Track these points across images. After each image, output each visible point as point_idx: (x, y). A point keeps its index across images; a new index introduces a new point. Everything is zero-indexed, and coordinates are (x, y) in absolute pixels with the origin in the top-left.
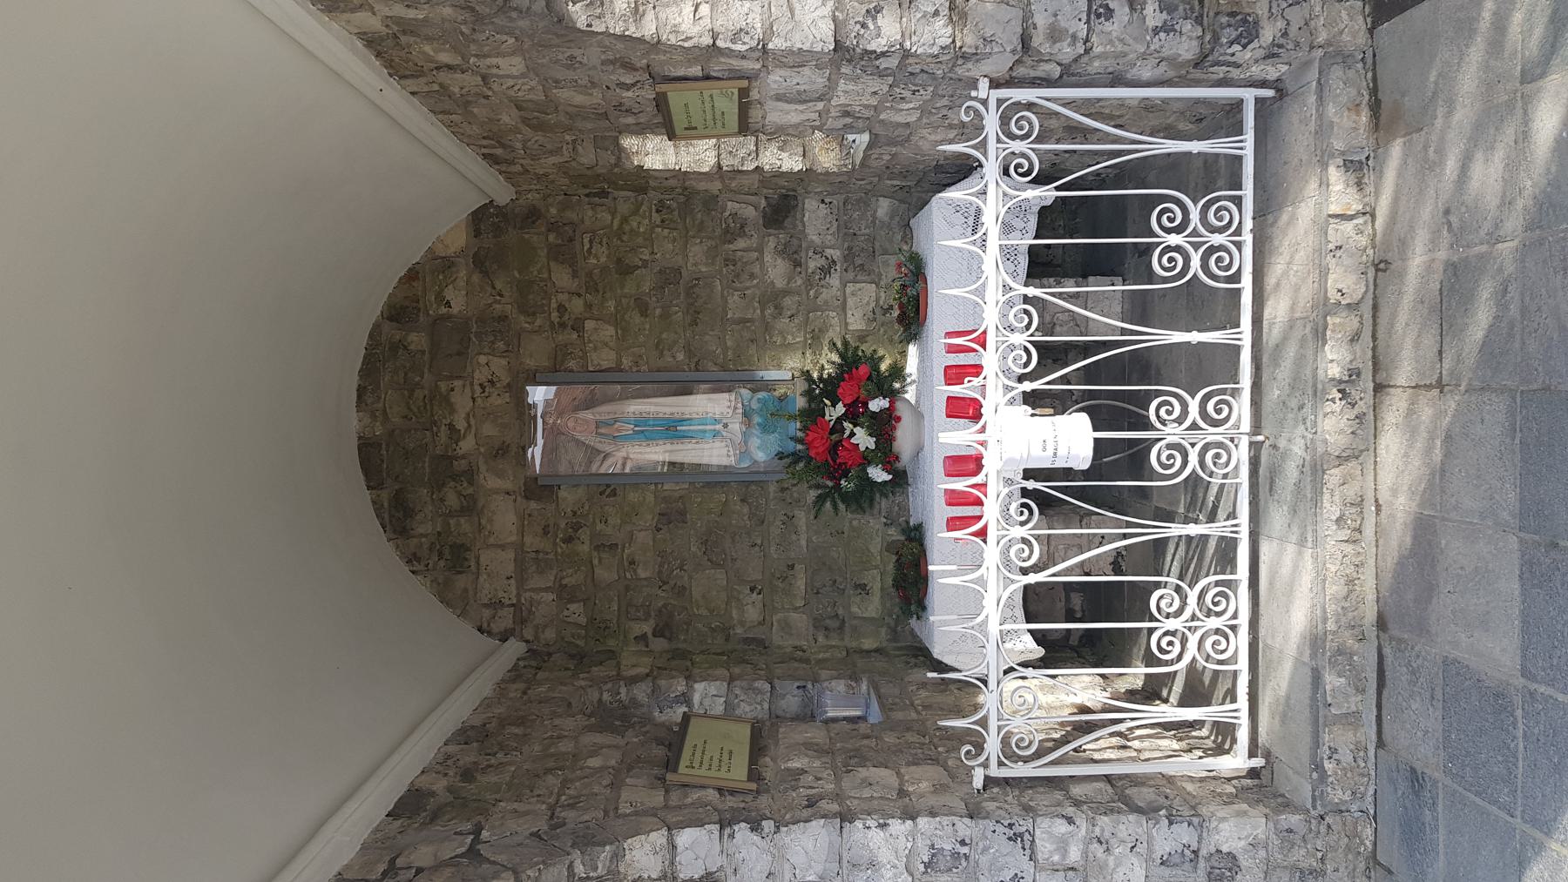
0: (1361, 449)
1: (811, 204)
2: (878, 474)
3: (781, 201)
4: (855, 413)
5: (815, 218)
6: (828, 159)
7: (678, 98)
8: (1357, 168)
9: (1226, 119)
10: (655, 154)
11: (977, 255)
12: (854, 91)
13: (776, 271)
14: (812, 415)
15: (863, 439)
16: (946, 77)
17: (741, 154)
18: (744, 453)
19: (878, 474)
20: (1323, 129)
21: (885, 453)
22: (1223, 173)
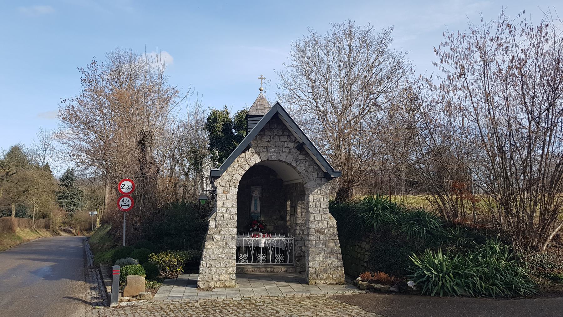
0: (261, 272)
1: (283, 222)
2: (251, 229)
3: (283, 218)
4: (258, 226)
5: (281, 222)
6: (288, 224)
7: (293, 209)
8: (286, 271)
9: (291, 261)
10: (289, 203)
11: (278, 239)
12: (294, 225)
13: (274, 217)
14: (258, 221)
15: (256, 227)
16: (294, 234)
17: (289, 213)
18: (252, 213)
19: (251, 229)
20: (289, 268)
21: (254, 230)
22: (286, 261)
